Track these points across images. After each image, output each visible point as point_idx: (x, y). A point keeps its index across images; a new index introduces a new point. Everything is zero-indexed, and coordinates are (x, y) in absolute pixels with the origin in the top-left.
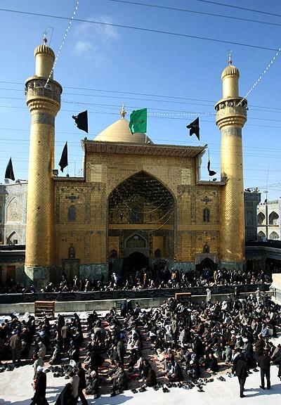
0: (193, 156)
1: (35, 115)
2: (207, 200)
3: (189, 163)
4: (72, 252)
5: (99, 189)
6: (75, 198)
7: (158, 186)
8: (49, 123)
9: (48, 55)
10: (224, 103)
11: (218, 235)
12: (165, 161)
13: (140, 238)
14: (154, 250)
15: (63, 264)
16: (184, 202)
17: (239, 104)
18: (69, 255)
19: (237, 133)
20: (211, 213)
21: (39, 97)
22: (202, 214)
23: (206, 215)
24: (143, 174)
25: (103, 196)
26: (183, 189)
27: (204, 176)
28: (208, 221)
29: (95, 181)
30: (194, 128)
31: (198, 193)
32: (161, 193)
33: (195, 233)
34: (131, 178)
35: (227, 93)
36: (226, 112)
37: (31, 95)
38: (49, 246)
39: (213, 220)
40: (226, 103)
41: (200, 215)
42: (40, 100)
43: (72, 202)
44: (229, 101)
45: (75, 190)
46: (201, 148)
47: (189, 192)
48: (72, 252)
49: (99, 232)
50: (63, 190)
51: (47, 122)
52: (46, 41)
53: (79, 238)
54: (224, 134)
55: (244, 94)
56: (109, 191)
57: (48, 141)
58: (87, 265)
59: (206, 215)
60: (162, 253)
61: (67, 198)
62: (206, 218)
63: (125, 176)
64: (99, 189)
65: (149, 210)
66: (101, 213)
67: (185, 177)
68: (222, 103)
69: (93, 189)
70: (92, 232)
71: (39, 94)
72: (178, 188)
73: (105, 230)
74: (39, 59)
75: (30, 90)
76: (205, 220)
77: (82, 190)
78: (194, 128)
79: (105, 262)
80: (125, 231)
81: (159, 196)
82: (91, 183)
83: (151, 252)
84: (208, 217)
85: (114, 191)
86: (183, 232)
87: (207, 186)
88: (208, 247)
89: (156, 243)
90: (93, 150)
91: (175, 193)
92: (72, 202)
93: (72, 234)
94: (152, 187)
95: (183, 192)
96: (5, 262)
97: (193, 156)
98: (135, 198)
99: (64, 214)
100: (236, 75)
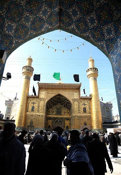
0: (78, 88)
1: (24, 76)
2: (85, 104)
3: (77, 91)
4: (32, 123)
6: (34, 103)
7: (66, 100)
8: (28, 79)
9: (30, 60)
10: (88, 70)
11: (90, 118)
12: (68, 91)
13: (60, 121)
14: (66, 126)
15: (28, 127)
16: (75, 106)
17: (96, 70)
18: (30, 124)
19: (95, 79)
20: (87, 109)
21: (26, 71)
22: (83, 110)
23: (85, 110)
24: (59, 95)
26: (75, 100)
27: (82, 95)
28: (86, 112)
29: (42, 97)
30: (76, 78)
31: (81, 101)
32: (67, 102)
33: (80, 117)
34: (55, 96)
35: (90, 66)
36: (90, 72)
37: (24, 71)
38: (23, 120)
40: (89, 70)
41: (82, 110)
42: (26, 72)
44: (91, 69)
45: (34, 100)
46: (79, 84)
47: (77, 101)
48: (32, 123)
49: (42, 116)
50: (31, 100)
51: (28, 78)
53: (35, 118)
54: (90, 81)
55: (95, 67)
56: (46, 101)
57: (27, 85)
58: (36, 128)
59: (85, 110)
60: (69, 128)
63: (53, 95)
64: (43, 100)
65: (64, 110)
67: (76, 96)
68: (90, 69)
70: (39, 116)
71: (26, 70)
72: (73, 100)
73: (44, 115)
74: (28, 61)
75: (23, 69)
76: (84, 112)
77: (37, 100)
78: (76, 78)
79: (43, 128)
80: (54, 118)
81: (67, 105)
83: (64, 127)
84: (86, 111)
85: (48, 101)
86: (75, 117)
87: (84, 99)
89: (67, 123)
90: (41, 87)
91: (72, 102)
94: (63, 100)
95: (75, 101)
98: (59, 106)
99: (30, 108)
100: (93, 61)
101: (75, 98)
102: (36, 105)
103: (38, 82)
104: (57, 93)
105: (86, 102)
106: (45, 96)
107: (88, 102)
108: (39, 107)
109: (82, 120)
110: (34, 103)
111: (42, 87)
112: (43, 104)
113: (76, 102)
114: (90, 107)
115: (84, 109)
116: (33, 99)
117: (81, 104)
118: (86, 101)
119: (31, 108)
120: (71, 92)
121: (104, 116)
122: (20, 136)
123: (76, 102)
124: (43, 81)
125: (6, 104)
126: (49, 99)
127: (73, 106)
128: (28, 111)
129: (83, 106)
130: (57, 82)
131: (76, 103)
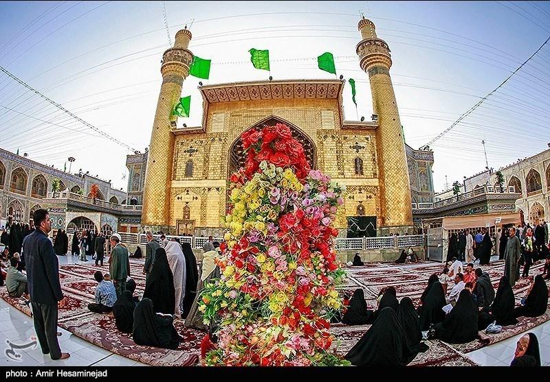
2: (358, 148)
5: (220, 140)
16: (327, 152)
23: (359, 166)
24: (273, 121)
25: (223, 147)
26: (324, 134)
28: (362, 174)
30: (326, 62)
31: (345, 138)
39: (368, 172)
41: (349, 168)
43: (190, 155)
45: (194, 142)
47: (333, 137)
52: (186, 27)
56: (231, 141)
59: (359, 166)
61: (185, 152)
62: (359, 169)
64: (220, 140)
66: (222, 167)
67: (328, 120)
69: (213, 140)
72: (318, 133)
76: (357, 173)
82: (211, 134)
84: (361, 168)
88: (363, 209)
91: (315, 140)
92: (190, 155)
93: (188, 191)
95: (326, 137)
96: (130, 223)
97: (329, 94)
101: (327, 126)
102: (198, 159)
103: (201, 83)
104: (267, 115)
105: (363, 141)
106: (230, 126)
107: (367, 139)
108: (206, 161)
109: (350, 197)
110: (191, 151)
111: (215, 98)
112: (219, 152)
113: (329, 139)
114: (374, 155)
115: (356, 164)
116: (190, 138)
117: (346, 145)
118: (362, 137)
119: (184, 166)
120: (311, 112)
121: (415, 189)
122: (89, 248)
123: (329, 139)
124: (218, 77)
125: (128, 165)
126: (237, 134)
127: (318, 152)
128: (175, 176)
129: (353, 155)
130: (261, 76)
131: (330, 143)
